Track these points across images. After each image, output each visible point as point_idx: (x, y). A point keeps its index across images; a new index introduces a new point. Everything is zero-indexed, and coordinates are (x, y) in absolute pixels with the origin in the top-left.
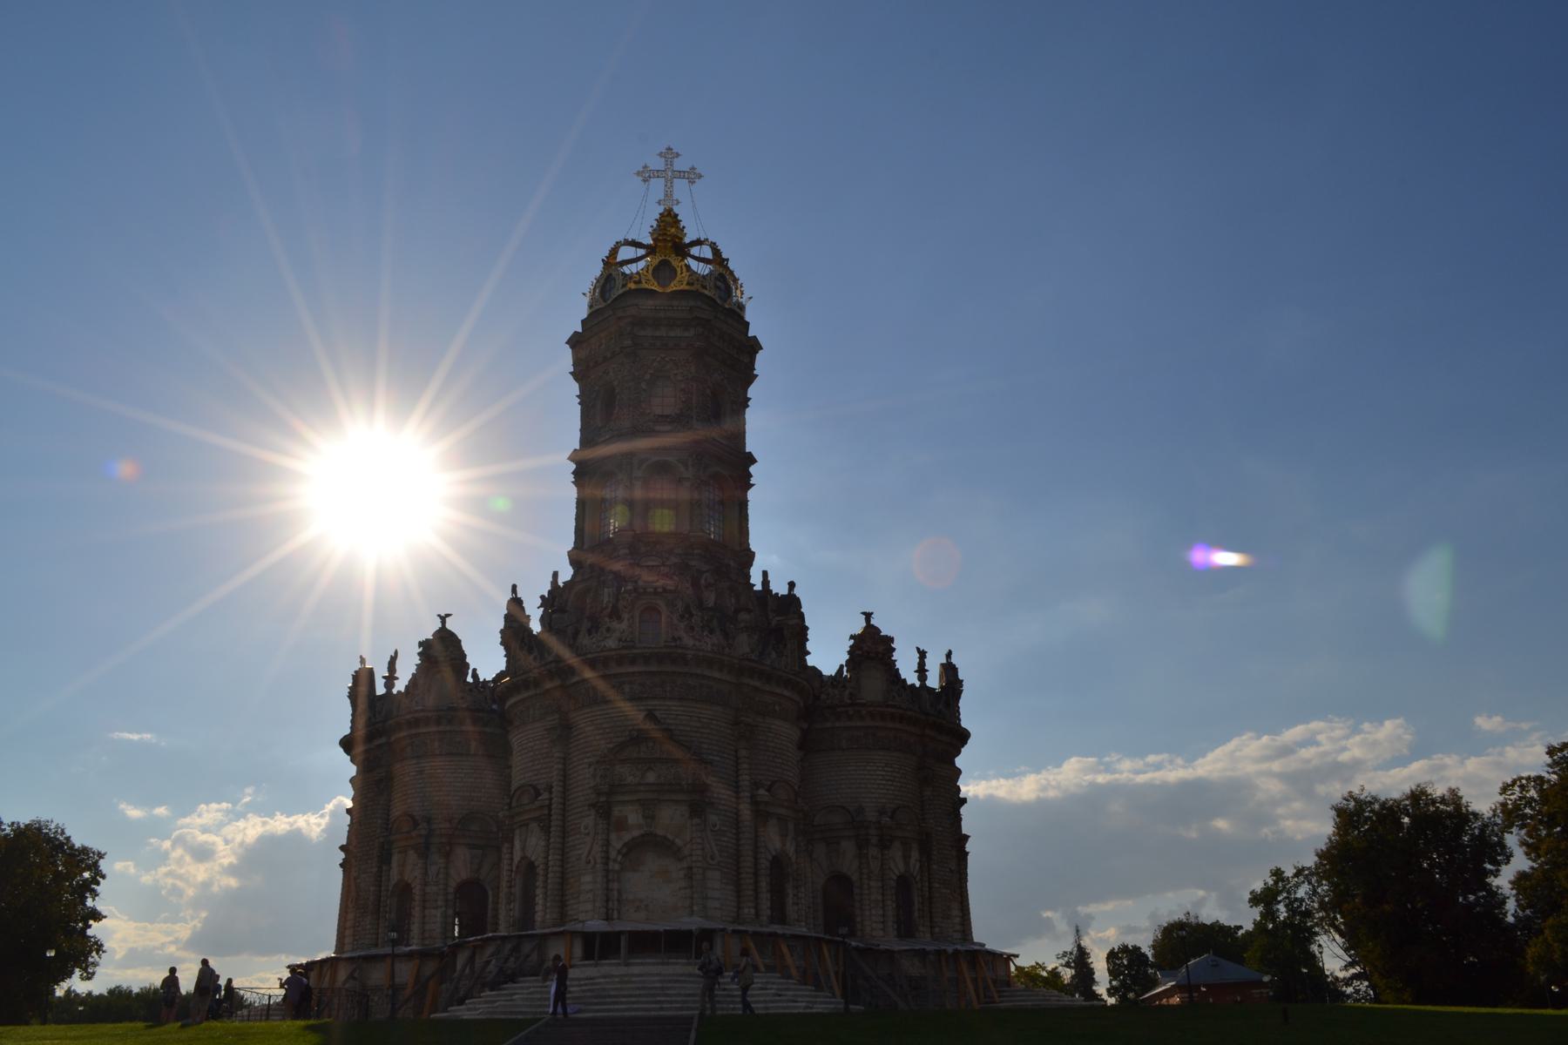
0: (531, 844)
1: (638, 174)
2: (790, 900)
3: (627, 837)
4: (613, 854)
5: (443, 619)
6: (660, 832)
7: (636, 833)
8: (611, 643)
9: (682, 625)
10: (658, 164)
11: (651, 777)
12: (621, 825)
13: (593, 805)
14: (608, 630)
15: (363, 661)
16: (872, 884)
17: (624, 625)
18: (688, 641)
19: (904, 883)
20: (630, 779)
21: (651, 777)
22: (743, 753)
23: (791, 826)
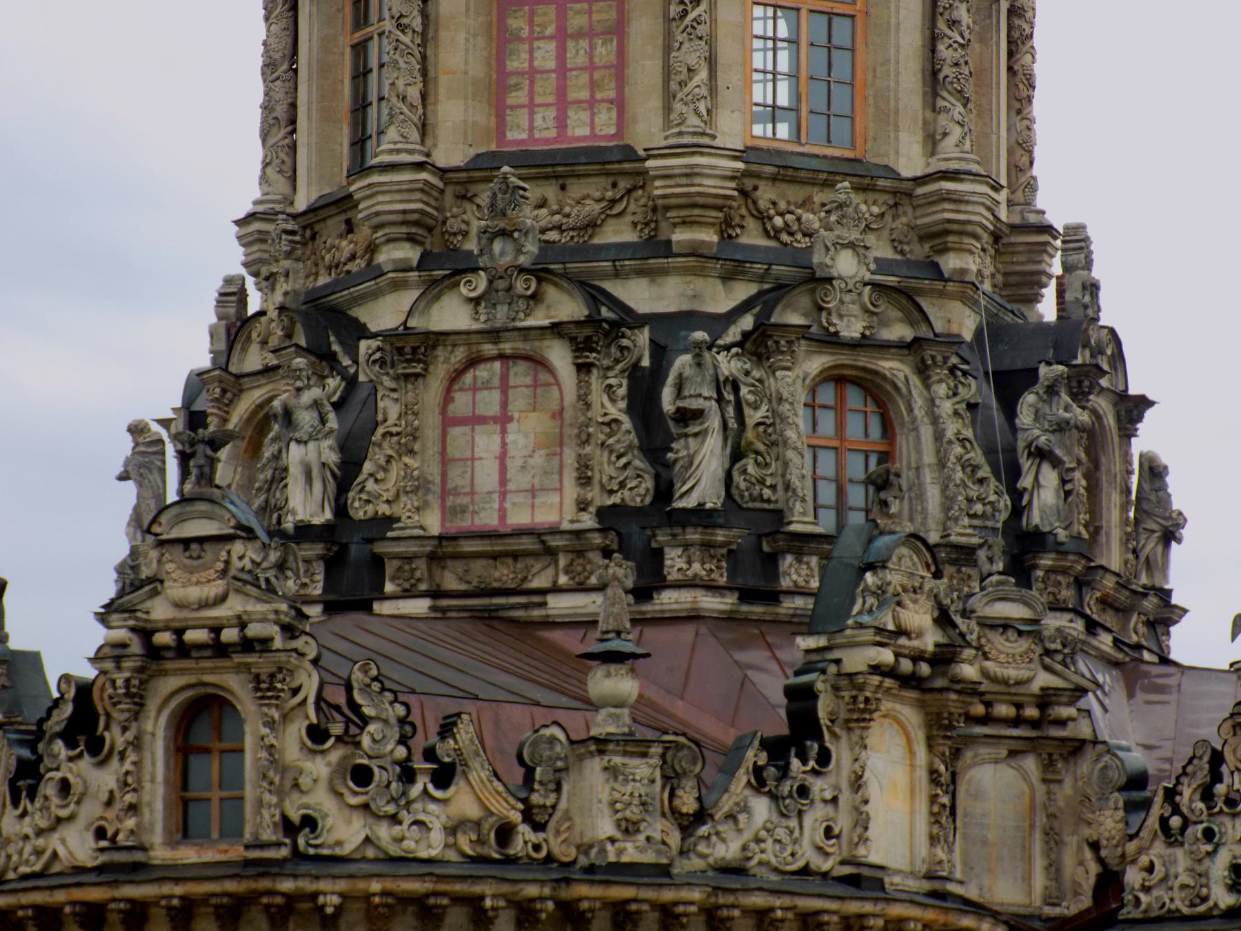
8: (76, 846)
9: (319, 768)
14: (65, 787)
17: (105, 779)
18: (345, 831)
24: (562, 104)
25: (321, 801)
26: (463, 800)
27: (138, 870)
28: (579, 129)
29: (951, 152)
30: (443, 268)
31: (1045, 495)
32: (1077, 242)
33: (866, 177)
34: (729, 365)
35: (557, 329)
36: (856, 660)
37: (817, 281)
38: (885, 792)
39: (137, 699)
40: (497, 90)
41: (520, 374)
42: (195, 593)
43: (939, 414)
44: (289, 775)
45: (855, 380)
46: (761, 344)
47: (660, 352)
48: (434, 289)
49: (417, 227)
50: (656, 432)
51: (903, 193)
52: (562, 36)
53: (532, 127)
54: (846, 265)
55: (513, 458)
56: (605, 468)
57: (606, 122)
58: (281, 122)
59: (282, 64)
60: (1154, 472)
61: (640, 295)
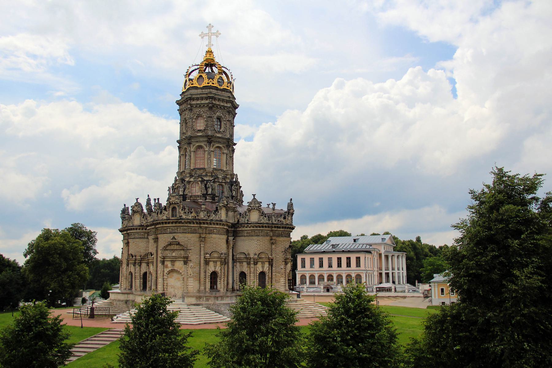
0: (152, 268)
1: (200, 35)
2: (218, 283)
3: (168, 270)
5: (137, 199)
8: (165, 218)
9: (182, 212)
10: (206, 31)
11: (174, 254)
12: (167, 267)
15: (125, 205)
17: (167, 213)
18: (184, 217)
19: (262, 274)
22: (202, 245)
23: (219, 263)
25: (182, 215)
26: (192, 215)
27: (169, 219)
28: (201, 167)
29: (228, 169)
30: (191, 176)
31: (234, 193)
33: (222, 170)
34: (212, 184)
36: (221, 205)
37: (218, 178)
38: (223, 215)
39: (169, 207)
40: (195, 164)
43: (226, 188)
44: (180, 212)
45: (221, 185)
46: (214, 182)
47: (207, 183)
48: (191, 178)
49: (190, 173)
50: (206, 188)
51: (224, 171)
53: (198, 166)
54: (220, 177)
55: (196, 190)
56: (203, 191)
58: (179, 165)
59: (180, 161)
60: (242, 191)
61: (205, 178)
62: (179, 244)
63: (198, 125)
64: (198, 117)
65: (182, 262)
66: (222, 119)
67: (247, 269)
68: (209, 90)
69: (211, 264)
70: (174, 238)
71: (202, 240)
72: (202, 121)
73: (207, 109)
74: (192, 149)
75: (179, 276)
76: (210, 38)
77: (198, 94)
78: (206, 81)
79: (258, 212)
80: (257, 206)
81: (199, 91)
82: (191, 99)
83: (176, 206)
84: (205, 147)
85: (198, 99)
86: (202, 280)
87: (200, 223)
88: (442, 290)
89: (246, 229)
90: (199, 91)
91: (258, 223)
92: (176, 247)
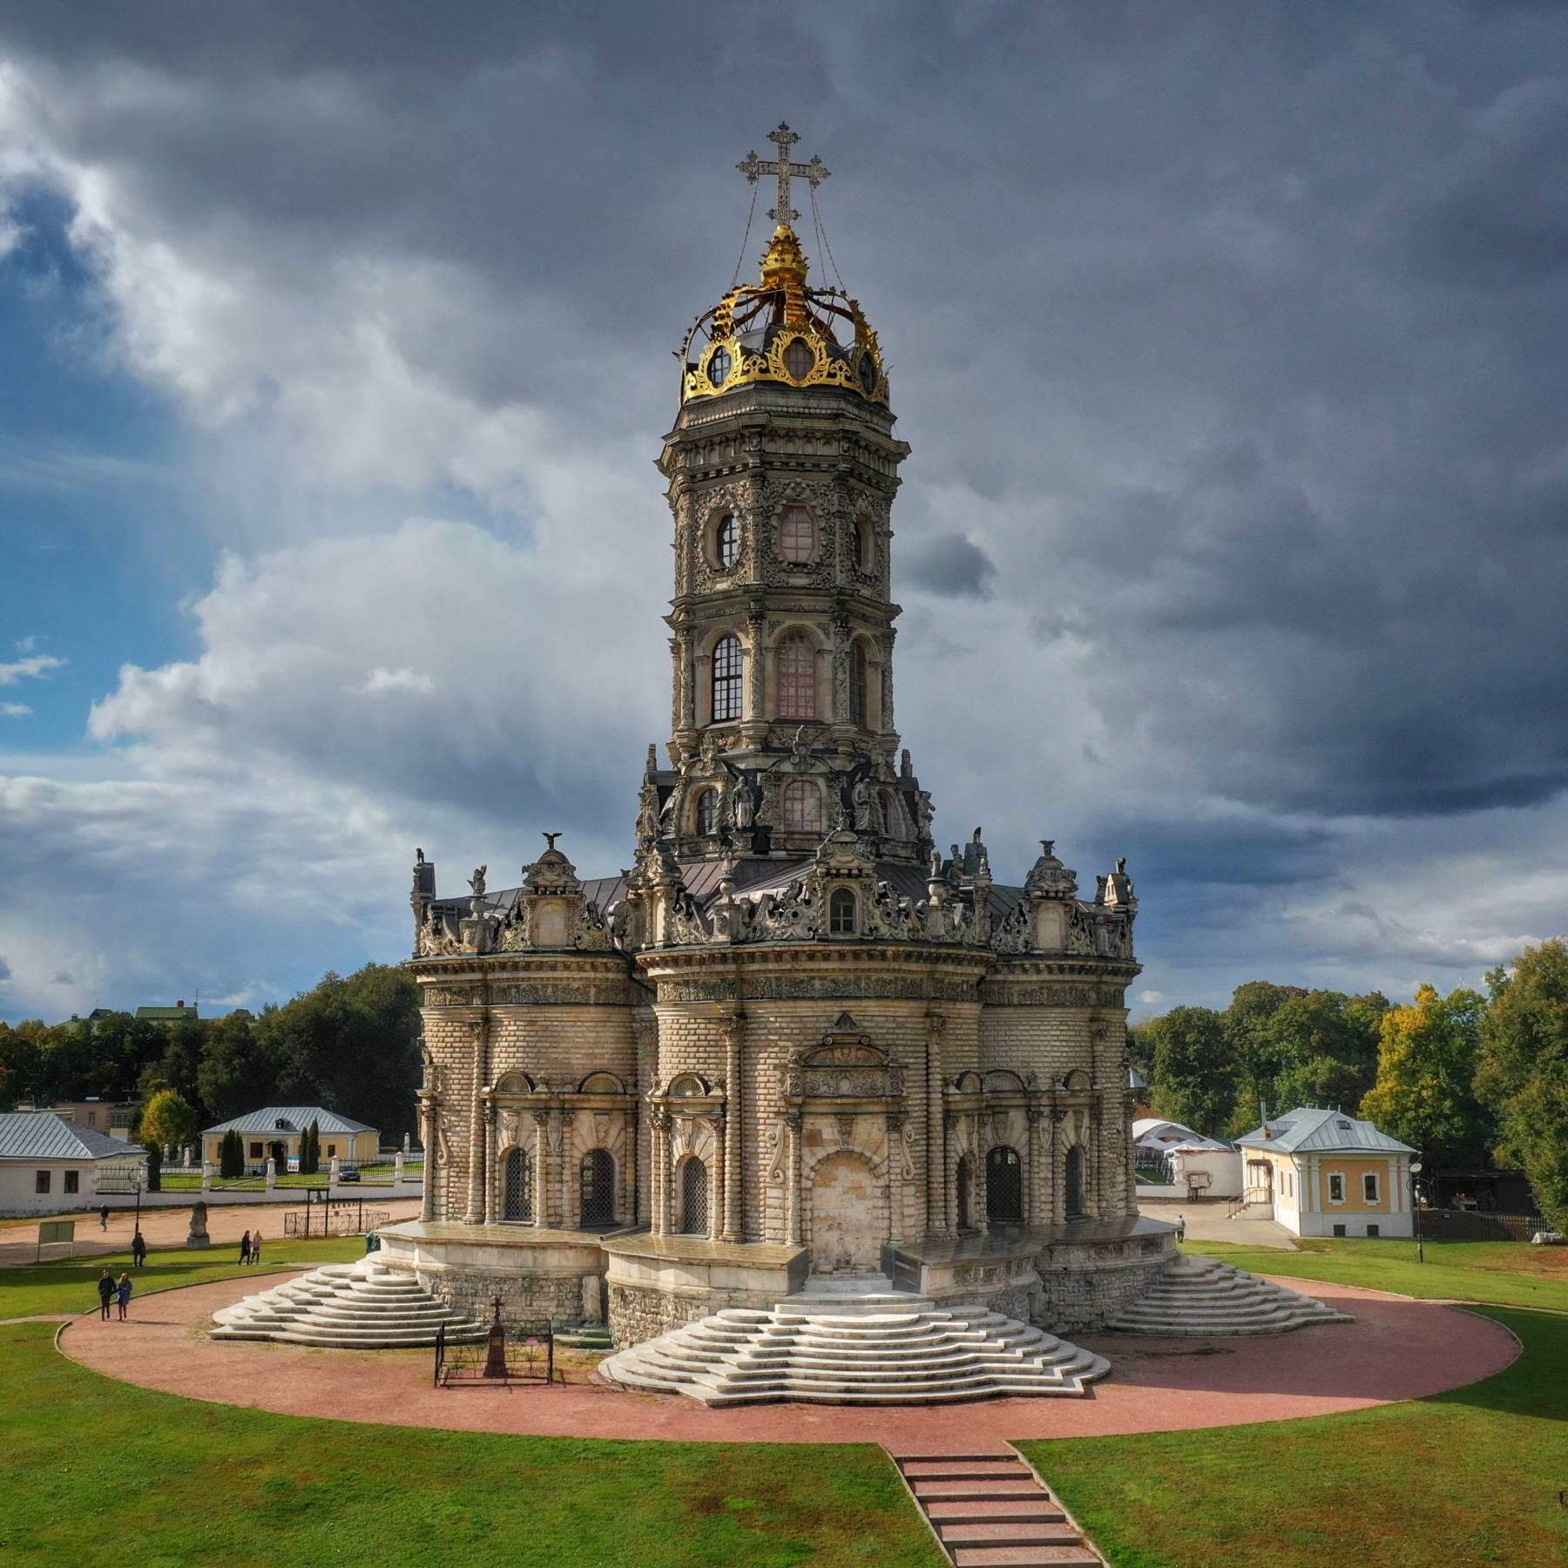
3: (821, 1153)
4: (806, 1171)
5: (551, 839)
6: (858, 1149)
7: (832, 1149)
9: (877, 912)
10: (769, 152)
11: (845, 1087)
12: (814, 1139)
13: (778, 1114)
14: (795, 915)
15: (420, 854)
16: (1043, 1160)
18: (884, 930)
19: (1074, 1153)
20: (824, 1089)
21: (845, 1087)
22: (934, 1049)
24: (797, 707)
28: (802, 713)
32: (906, 754)
35: (821, 775)
40: (778, 700)
41: (807, 787)
42: (845, 859)
52: (797, 687)
53: (789, 711)
57: (810, 713)
62: (864, 1042)
63: (789, 541)
64: (788, 509)
65: (880, 1122)
66: (869, 528)
67: (1025, 1137)
68: (834, 404)
69: (962, 1126)
70: (845, 1018)
71: (937, 1025)
72: (805, 528)
73: (826, 479)
74: (770, 642)
75: (863, 1178)
76: (784, 183)
77: (787, 415)
78: (823, 362)
79: (1061, 910)
80: (1062, 886)
81: (795, 403)
82: (765, 432)
83: (854, 886)
84: (823, 637)
85: (790, 435)
86: (938, 1190)
87: (937, 959)
88: (1336, 1183)
89: (1024, 978)
90: (795, 403)
91: (1066, 956)
92: (855, 1056)
